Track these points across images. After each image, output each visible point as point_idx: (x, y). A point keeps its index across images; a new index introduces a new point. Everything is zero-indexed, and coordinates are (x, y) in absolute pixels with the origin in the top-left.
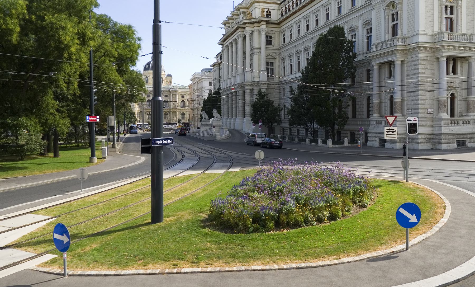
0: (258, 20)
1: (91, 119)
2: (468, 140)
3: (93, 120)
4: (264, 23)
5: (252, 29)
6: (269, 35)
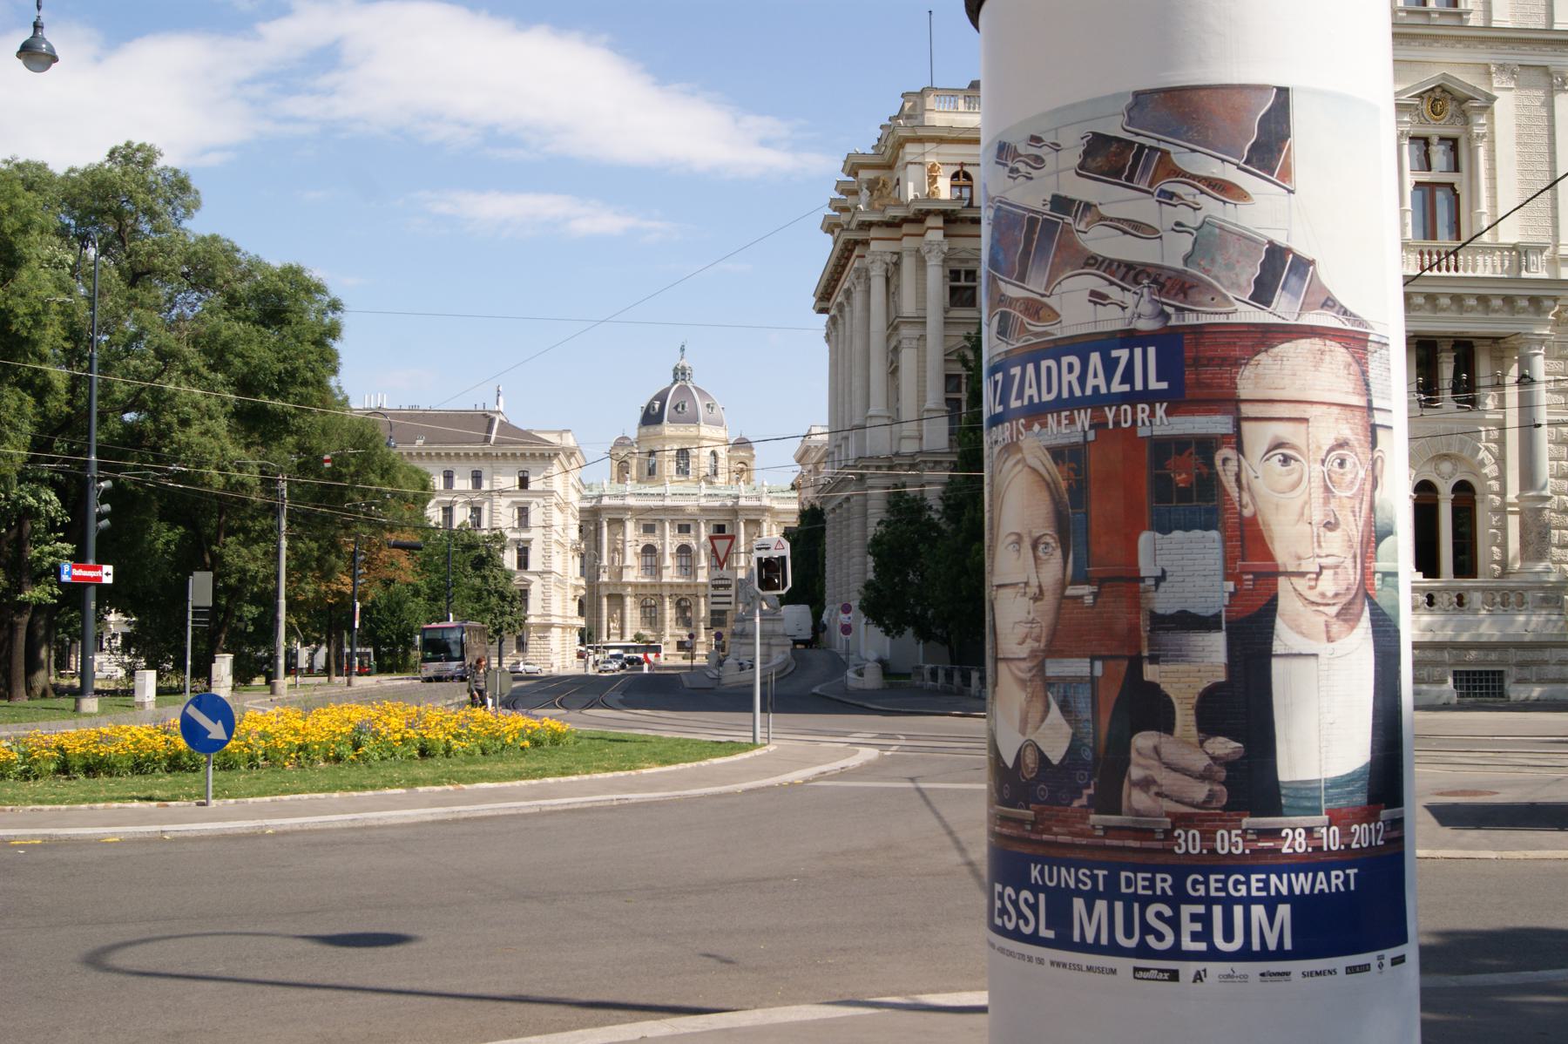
0: (913, 209)
1: (76, 572)
2: (1512, 673)
3: (88, 578)
4: (939, 222)
5: (893, 246)
6: (963, 267)
